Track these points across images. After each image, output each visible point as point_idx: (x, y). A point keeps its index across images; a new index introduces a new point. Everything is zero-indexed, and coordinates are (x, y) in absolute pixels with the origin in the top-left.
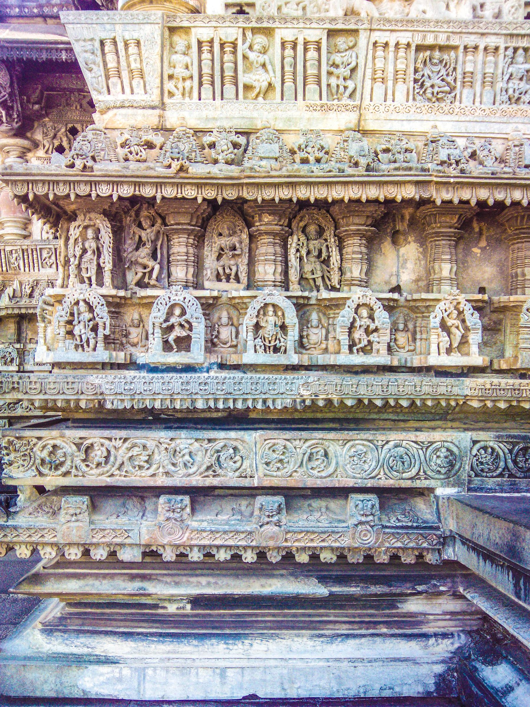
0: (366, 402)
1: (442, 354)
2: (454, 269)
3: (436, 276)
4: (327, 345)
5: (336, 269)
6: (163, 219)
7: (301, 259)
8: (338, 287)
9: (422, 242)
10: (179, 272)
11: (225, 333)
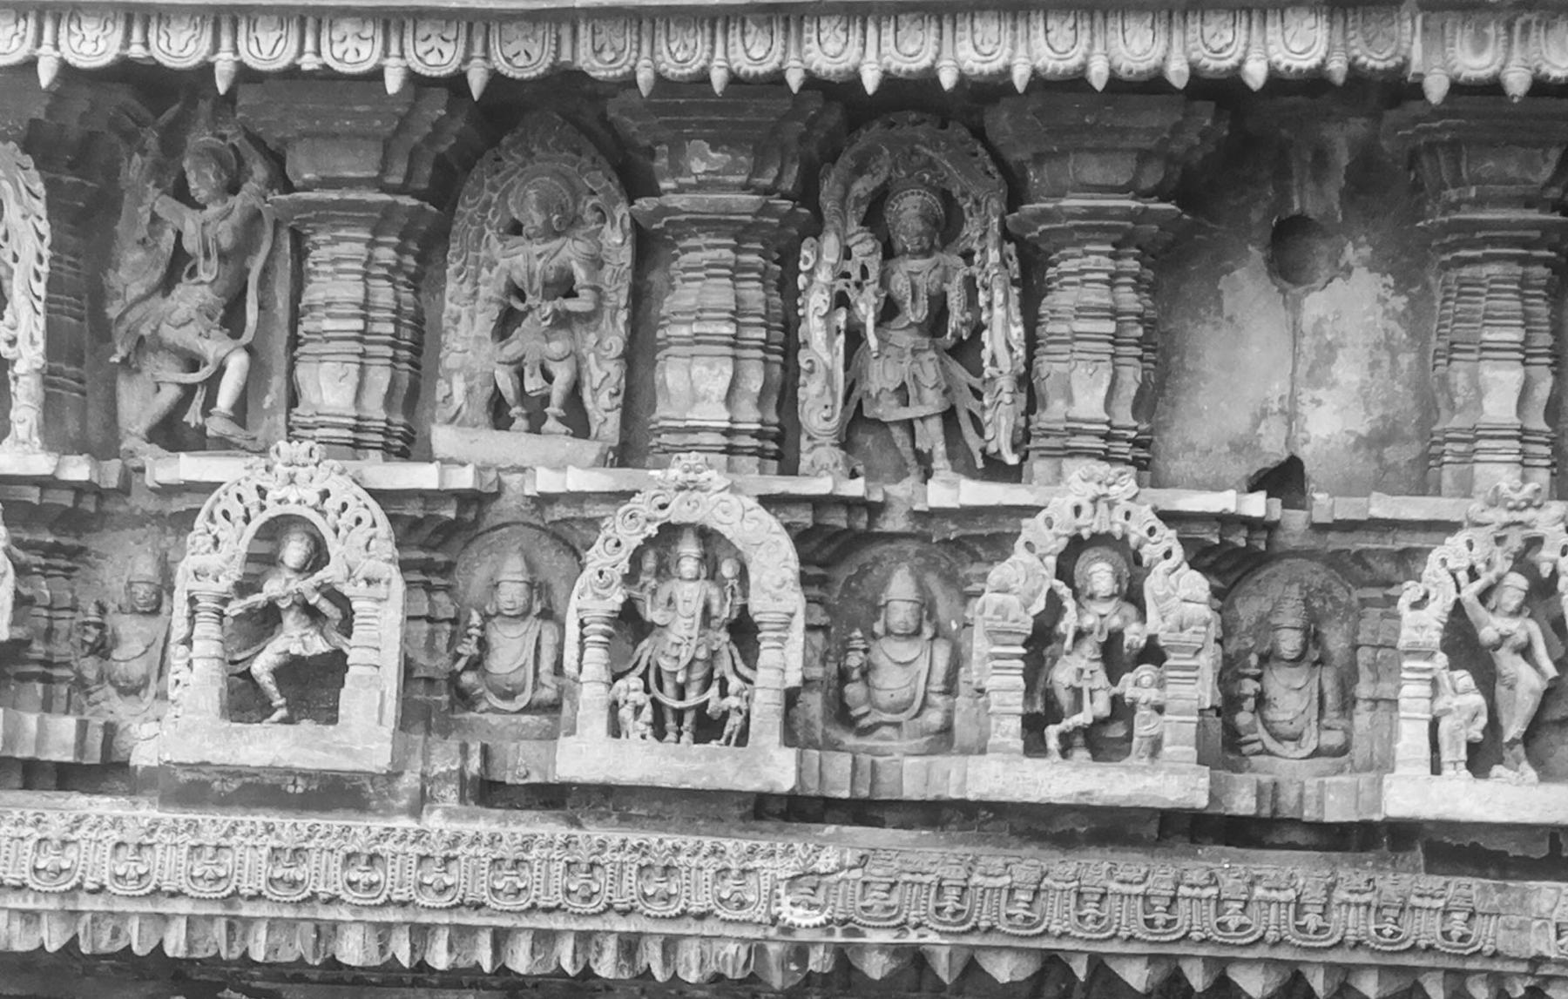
0: (1080, 969)
1: (1448, 771)
2: (1544, 388)
3: (1457, 421)
4: (949, 714)
5: (1006, 383)
6: (276, 159)
7: (854, 337)
8: (1012, 460)
9: (1408, 263)
10: (329, 388)
11: (511, 651)
